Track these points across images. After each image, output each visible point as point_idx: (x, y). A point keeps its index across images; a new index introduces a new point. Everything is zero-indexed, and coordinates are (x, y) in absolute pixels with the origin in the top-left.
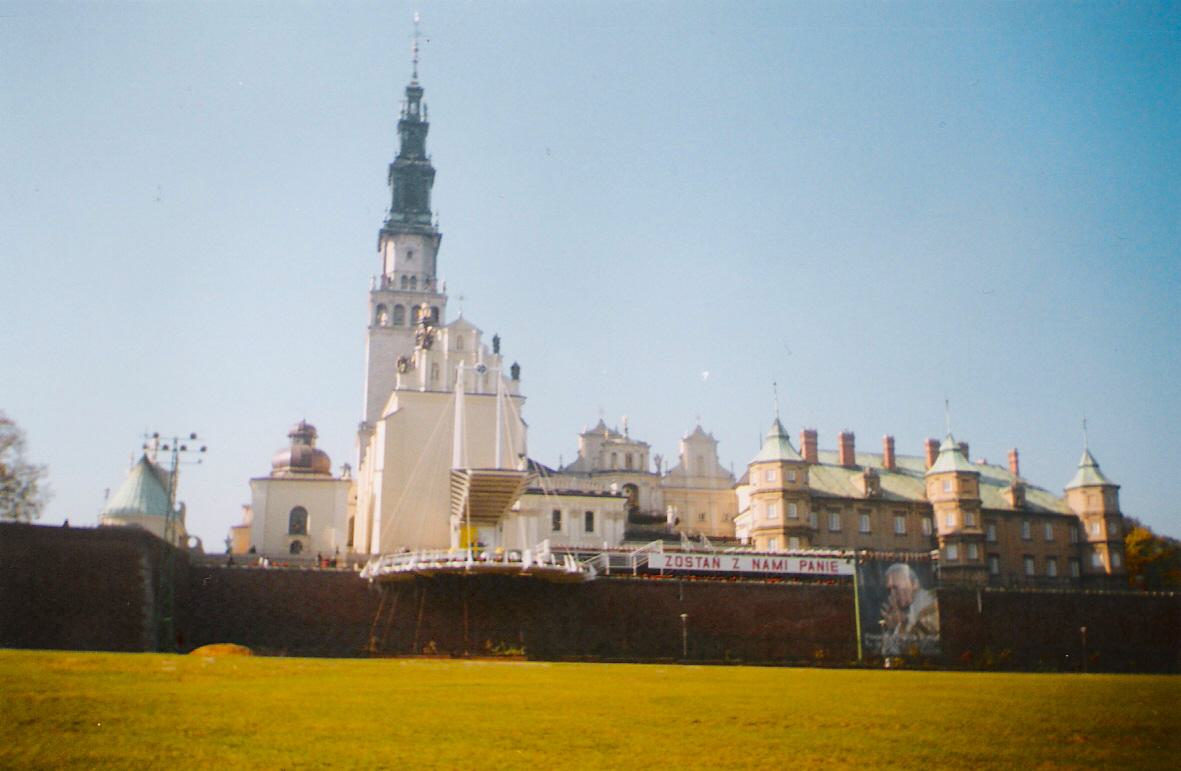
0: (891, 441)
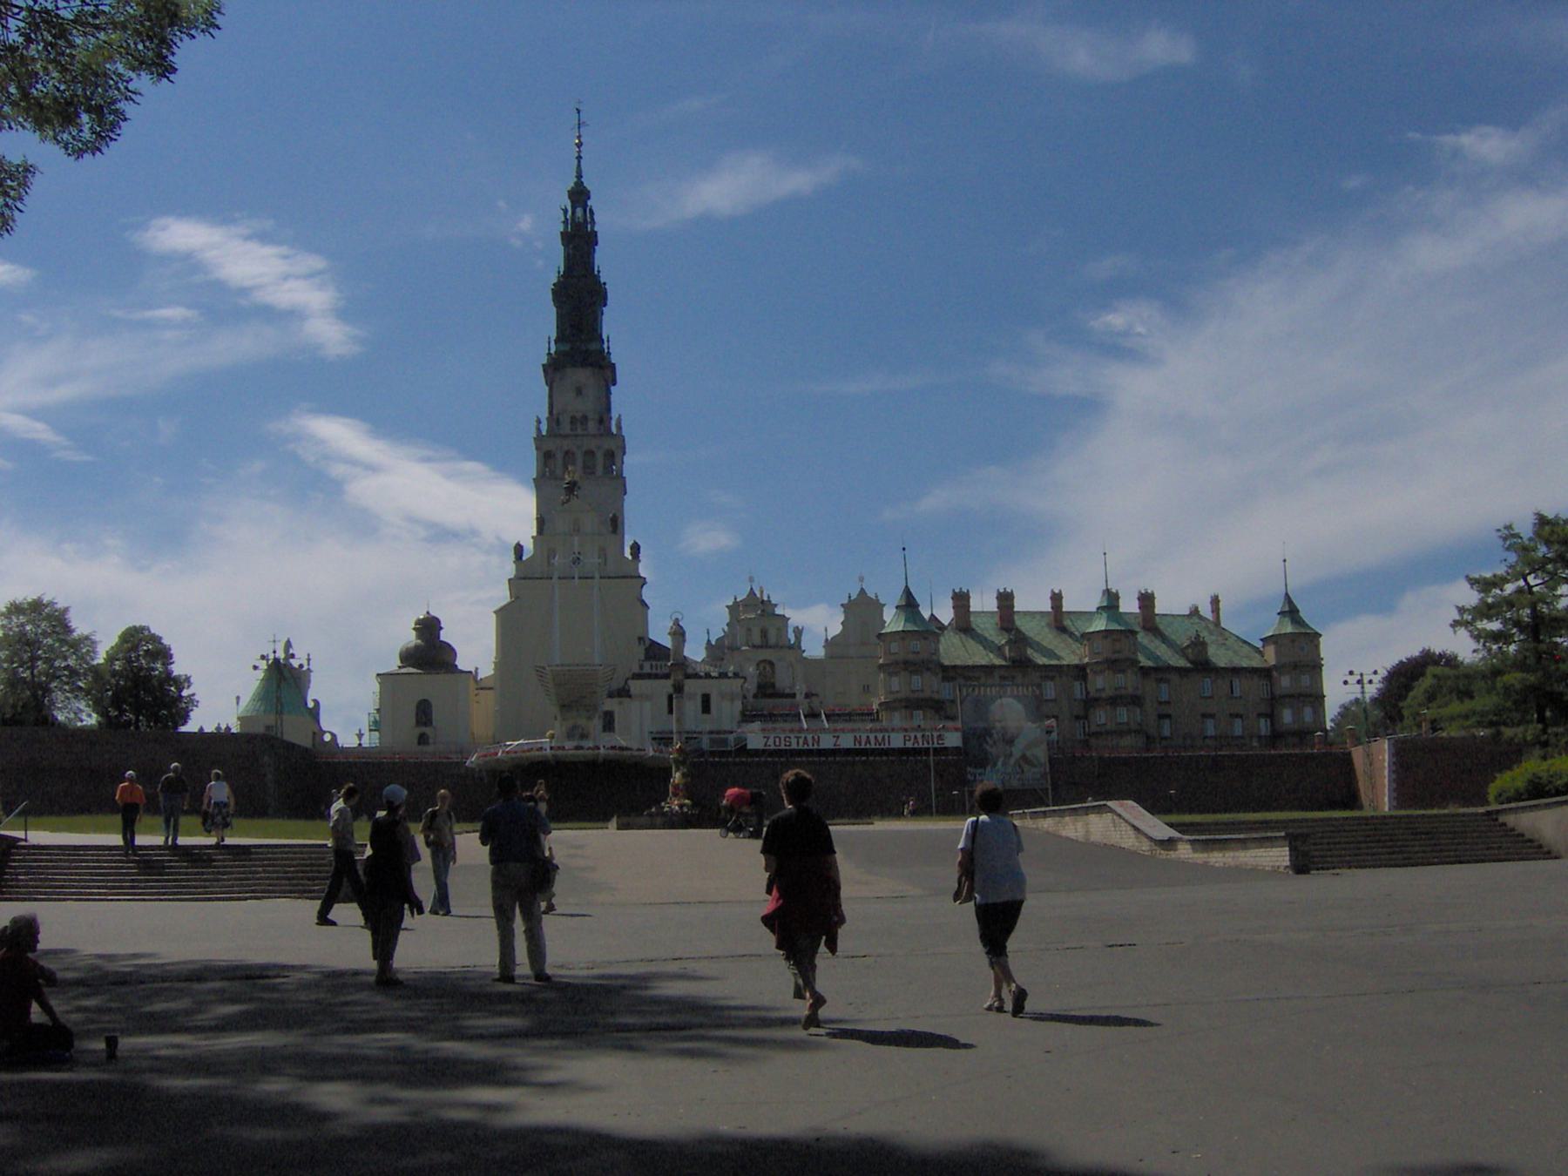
0: (1057, 598)
